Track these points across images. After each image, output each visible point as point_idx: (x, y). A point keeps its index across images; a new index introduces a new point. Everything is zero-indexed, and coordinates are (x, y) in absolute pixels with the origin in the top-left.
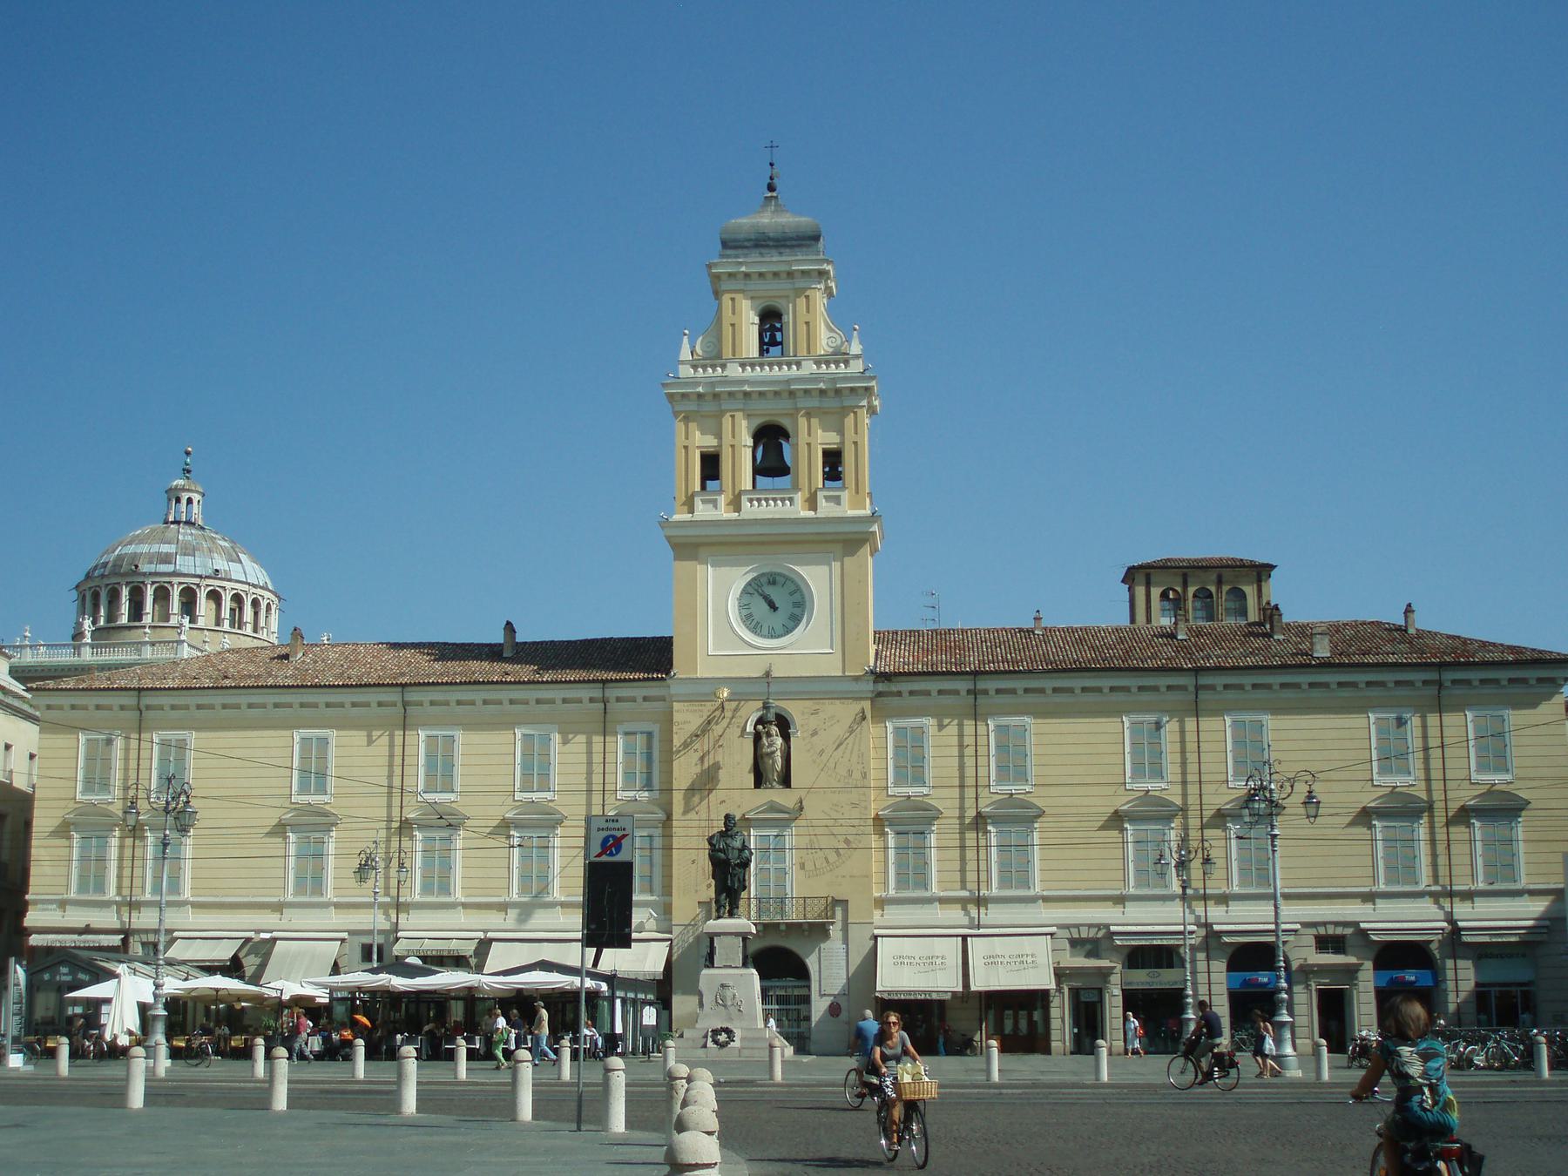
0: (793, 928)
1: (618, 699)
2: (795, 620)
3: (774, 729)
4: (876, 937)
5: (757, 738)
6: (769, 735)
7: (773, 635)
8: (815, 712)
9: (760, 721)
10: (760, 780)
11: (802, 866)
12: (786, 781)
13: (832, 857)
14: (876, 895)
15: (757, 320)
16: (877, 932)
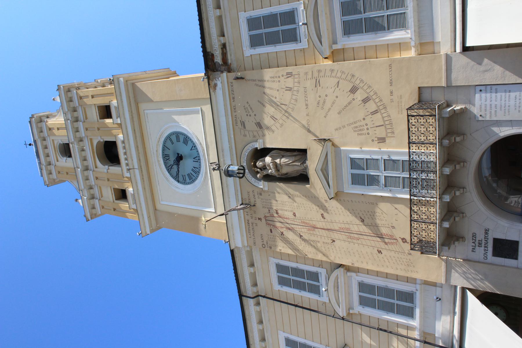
0: (450, 157)
1: (255, 285)
2: (187, 139)
3: (259, 164)
4: (465, 49)
5: (268, 178)
6: (264, 168)
7: (197, 159)
8: (243, 124)
9: (254, 174)
10: (303, 178)
11: (382, 140)
12: (302, 153)
13: (372, 106)
14: (412, 53)
15: (65, 158)
16: (459, 49)
